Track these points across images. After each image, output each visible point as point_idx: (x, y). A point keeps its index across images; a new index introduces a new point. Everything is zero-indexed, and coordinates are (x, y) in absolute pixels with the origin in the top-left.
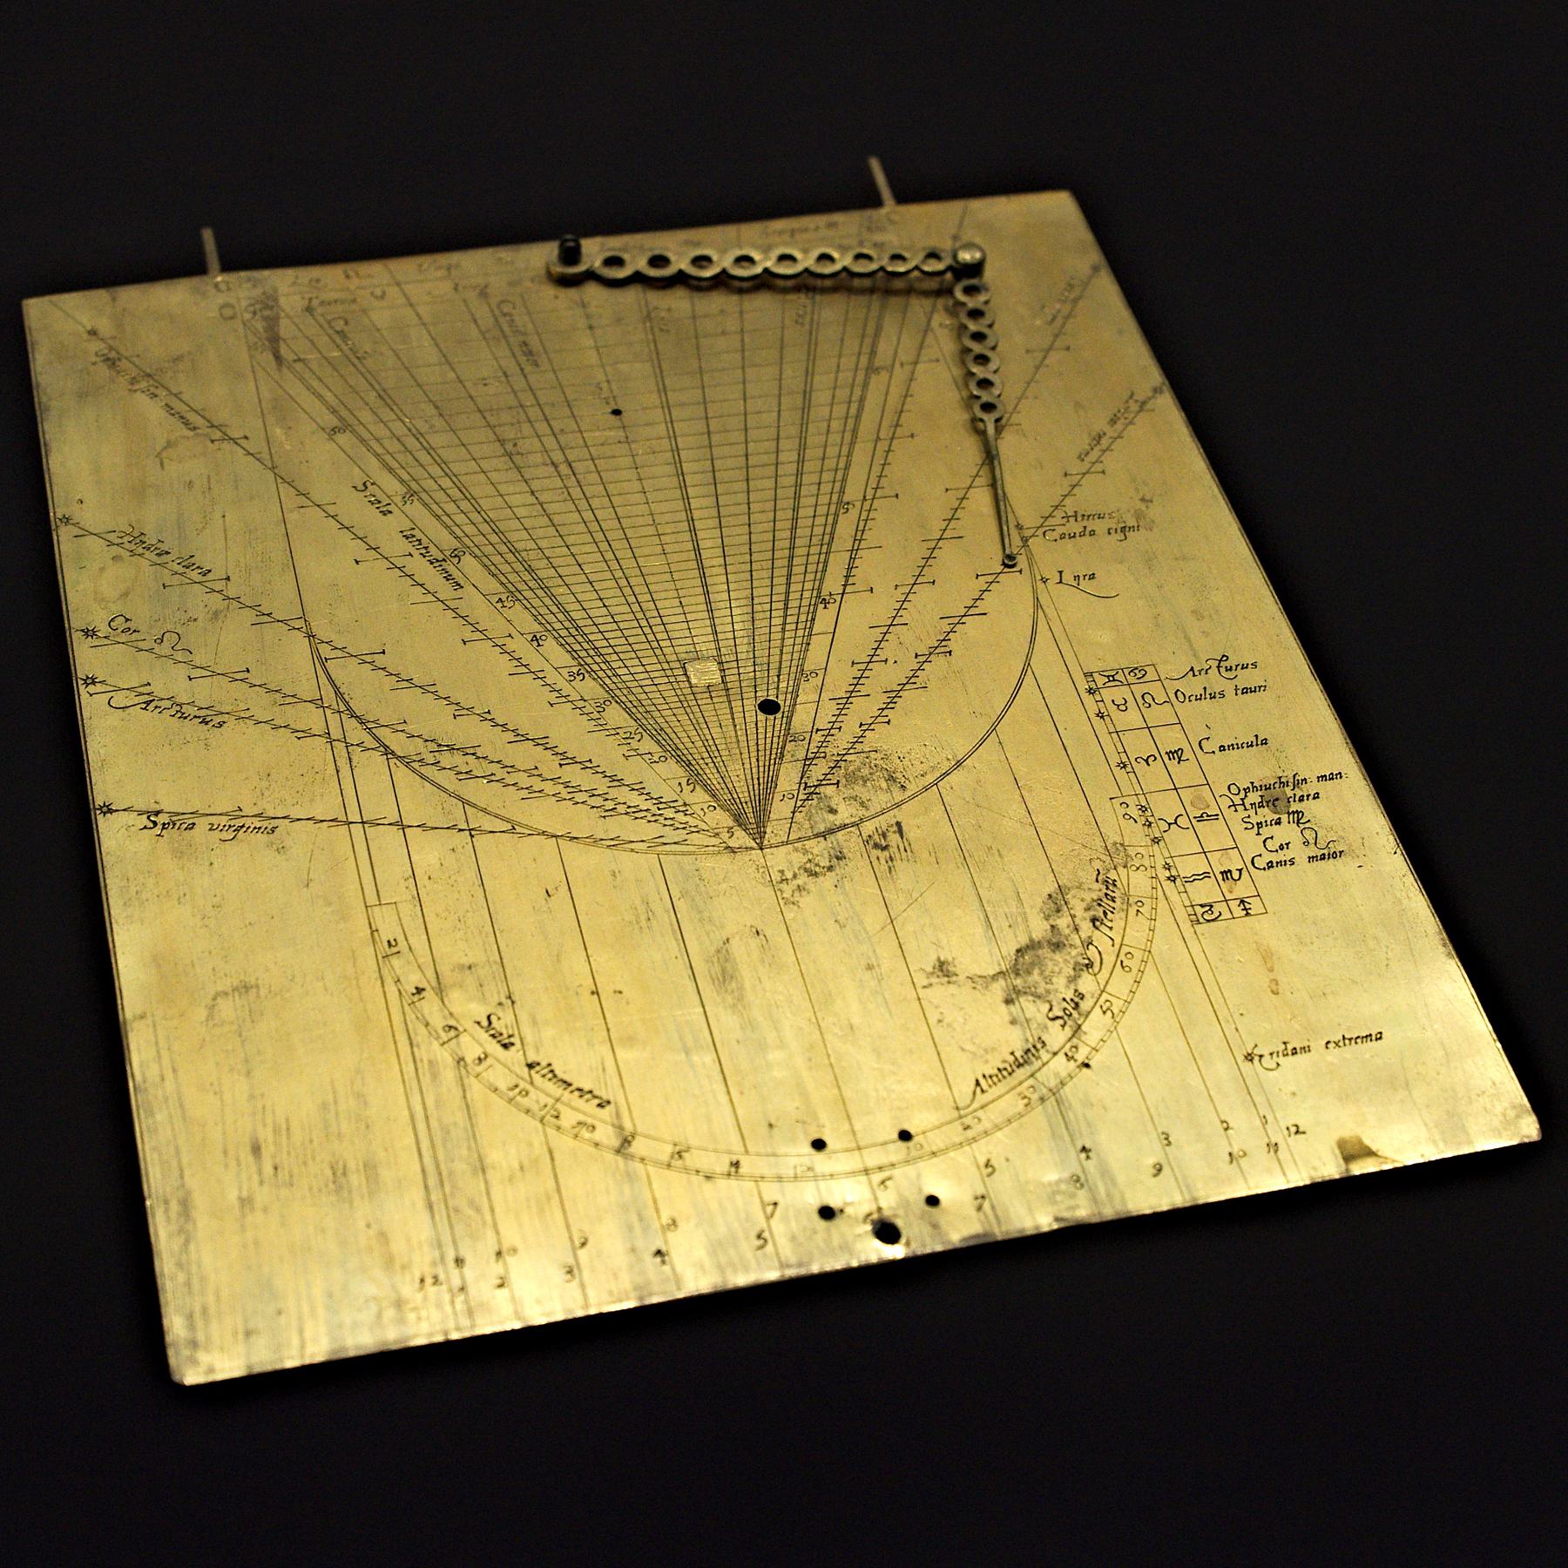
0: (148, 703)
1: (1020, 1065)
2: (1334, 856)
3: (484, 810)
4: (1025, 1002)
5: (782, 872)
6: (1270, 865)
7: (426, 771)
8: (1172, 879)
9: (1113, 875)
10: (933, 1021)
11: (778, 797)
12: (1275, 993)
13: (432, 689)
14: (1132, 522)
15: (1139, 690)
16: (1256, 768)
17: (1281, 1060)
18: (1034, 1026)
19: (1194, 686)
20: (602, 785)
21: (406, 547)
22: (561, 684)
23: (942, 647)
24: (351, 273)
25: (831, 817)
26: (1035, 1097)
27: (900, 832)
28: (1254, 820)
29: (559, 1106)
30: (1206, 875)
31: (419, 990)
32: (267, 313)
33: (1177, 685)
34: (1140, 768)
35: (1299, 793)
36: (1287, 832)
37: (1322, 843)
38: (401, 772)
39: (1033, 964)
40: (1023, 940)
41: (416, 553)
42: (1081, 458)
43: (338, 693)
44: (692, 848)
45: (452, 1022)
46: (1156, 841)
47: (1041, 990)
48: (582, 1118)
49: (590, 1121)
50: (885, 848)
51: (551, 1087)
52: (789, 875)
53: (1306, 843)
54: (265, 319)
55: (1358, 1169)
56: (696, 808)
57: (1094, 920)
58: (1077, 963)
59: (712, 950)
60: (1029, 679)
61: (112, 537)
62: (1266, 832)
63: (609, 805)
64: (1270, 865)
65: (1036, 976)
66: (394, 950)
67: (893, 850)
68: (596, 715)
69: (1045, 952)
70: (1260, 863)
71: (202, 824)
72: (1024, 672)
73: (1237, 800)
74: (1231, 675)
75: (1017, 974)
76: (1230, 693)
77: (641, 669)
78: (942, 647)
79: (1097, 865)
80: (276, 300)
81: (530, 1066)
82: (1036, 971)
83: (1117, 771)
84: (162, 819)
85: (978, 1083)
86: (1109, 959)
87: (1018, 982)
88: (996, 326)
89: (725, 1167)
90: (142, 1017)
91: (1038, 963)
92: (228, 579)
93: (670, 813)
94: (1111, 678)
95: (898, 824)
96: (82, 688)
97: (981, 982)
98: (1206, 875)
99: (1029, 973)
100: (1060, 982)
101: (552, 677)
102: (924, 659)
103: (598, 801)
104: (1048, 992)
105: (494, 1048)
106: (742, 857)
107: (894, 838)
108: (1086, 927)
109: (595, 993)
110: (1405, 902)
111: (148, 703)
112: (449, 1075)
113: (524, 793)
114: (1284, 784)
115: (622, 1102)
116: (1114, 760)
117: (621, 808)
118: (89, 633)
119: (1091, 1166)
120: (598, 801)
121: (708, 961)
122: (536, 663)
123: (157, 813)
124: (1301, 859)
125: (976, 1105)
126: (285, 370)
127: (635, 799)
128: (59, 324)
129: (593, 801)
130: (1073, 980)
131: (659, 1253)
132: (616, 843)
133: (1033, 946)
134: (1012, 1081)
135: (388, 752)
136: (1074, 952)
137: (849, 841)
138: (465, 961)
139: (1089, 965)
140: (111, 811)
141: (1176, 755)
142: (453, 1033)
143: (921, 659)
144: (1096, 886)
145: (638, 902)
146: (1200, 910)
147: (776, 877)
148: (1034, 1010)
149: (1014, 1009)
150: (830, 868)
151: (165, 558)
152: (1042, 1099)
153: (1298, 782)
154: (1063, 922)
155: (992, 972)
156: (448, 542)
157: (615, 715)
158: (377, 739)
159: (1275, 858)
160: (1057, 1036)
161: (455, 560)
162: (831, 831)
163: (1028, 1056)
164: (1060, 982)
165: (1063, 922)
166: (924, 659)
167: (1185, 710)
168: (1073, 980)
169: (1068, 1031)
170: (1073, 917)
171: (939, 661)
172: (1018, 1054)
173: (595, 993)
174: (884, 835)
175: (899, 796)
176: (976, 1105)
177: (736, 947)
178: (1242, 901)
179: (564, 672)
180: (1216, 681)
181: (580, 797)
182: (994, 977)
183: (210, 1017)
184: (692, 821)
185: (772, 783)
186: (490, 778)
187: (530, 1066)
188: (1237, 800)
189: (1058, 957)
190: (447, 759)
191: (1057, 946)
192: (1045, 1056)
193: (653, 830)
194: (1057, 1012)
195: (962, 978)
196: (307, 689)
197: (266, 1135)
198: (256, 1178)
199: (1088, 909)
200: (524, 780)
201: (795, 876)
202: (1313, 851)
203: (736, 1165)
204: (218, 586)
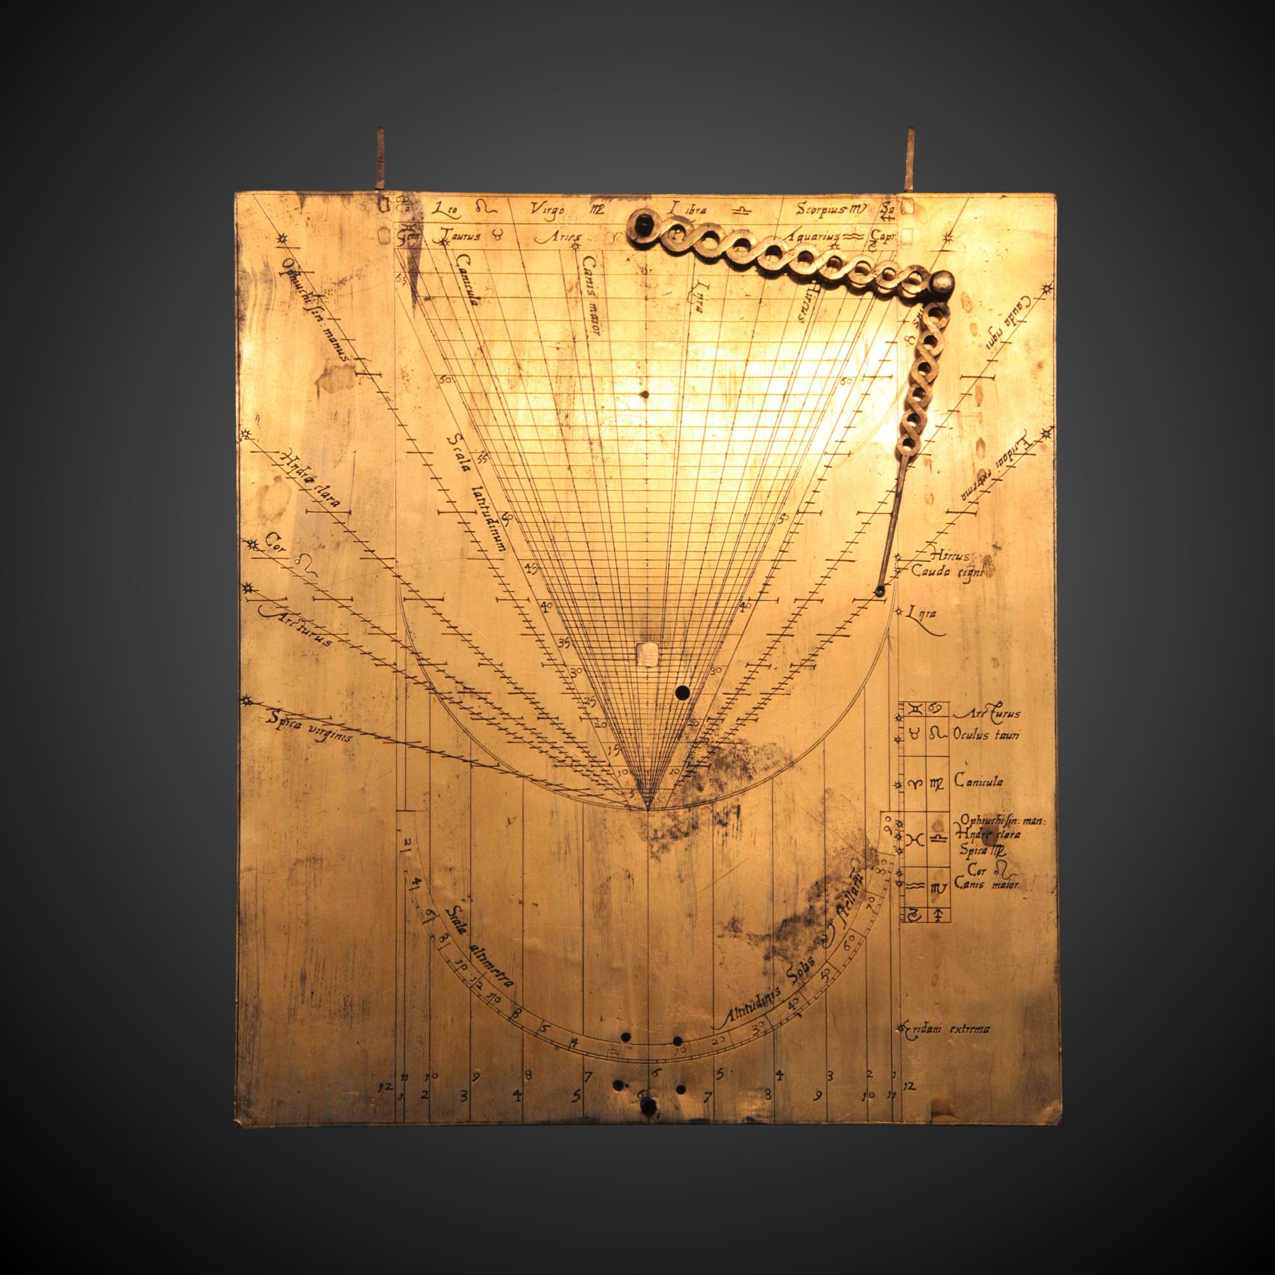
0: (284, 615)
1: (760, 1006)
2: (1011, 886)
3: (482, 747)
4: (777, 960)
5: (656, 831)
6: (966, 885)
7: (453, 708)
8: (899, 884)
9: (862, 874)
10: (717, 963)
11: (669, 770)
12: (934, 985)
13: (468, 638)
14: (979, 567)
15: (932, 722)
16: (985, 804)
17: (920, 1034)
18: (777, 977)
19: (969, 726)
20: (560, 739)
21: (473, 504)
22: (553, 649)
23: (809, 663)
24: (481, 204)
25: (698, 793)
26: (762, 1029)
27: (738, 813)
28: (969, 847)
29: (483, 980)
30: (921, 885)
31: (418, 881)
32: (412, 241)
33: (958, 723)
34: (909, 789)
35: (1007, 830)
36: (987, 860)
37: (1006, 874)
38: (437, 706)
39: (790, 933)
40: (790, 914)
41: (480, 511)
42: (964, 497)
43: (408, 632)
44: (606, 802)
45: (433, 908)
46: (900, 851)
47: (789, 953)
48: (495, 991)
49: (499, 995)
50: (725, 825)
51: (480, 965)
52: (660, 834)
53: (996, 872)
54: (410, 248)
55: (939, 1120)
56: (616, 769)
57: (839, 907)
58: (817, 938)
59: (599, 883)
60: (819, 749)
61: (276, 457)
62: (973, 858)
63: (562, 757)
64: (966, 885)
65: (789, 943)
66: (408, 847)
67: (729, 827)
68: (569, 680)
69: (800, 926)
70: (961, 882)
71: (306, 725)
72: (858, 695)
73: (964, 830)
74: (998, 720)
75: (778, 938)
76: (992, 736)
77: (607, 644)
78: (809, 663)
79: (855, 864)
80: (421, 229)
81: (472, 948)
82: (790, 939)
83: (893, 788)
84: (281, 716)
85: (731, 1014)
86: (838, 938)
87: (777, 944)
88: (940, 361)
89: (567, 1042)
90: (250, 869)
91: (793, 933)
92: (350, 513)
93: (598, 770)
94: (916, 709)
95: (739, 807)
96: (243, 592)
97: (755, 939)
98: (921, 885)
99: (786, 939)
100: (803, 949)
101: (548, 641)
102: (795, 669)
103: (555, 753)
104: (793, 956)
105: (453, 929)
106: (635, 815)
107: (733, 817)
108: (832, 910)
109: (521, 903)
110: (1044, 932)
111: (284, 615)
112: (423, 945)
113: (510, 738)
114: (999, 820)
115: (519, 983)
116: (895, 779)
117: (569, 761)
118: (252, 544)
119: (779, 1084)
120: (555, 753)
121: (594, 892)
122: (541, 629)
123: (279, 710)
124: (988, 886)
125: (724, 1029)
126: (419, 314)
127: (579, 755)
128: (261, 216)
129: (552, 752)
130: (811, 949)
131: (517, 1093)
132: (559, 789)
133: (795, 919)
134: (751, 1015)
135: (432, 689)
136: (818, 929)
137: (704, 815)
138: (449, 865)
139: (825, 941)
140: (250, 703)
141: (936, 782)
142: (432, 916)
143: (794, 668)
144: (849, 880)
145: (562, 839)
146: (908, 911)
147: (652, 834)
148: (779, 965)
149: (769, 964)
150: (687, 835)
151: (309, 485)
152: (766, 1032)
153: (1011, 821)
154: (819, 904)
155: (763, 933)
156: (503, 506)
157: (581, 682)
158: (426, 675)
159: (971, 879)
160: (788, 989)
161: (505, 523)
162: (695, 805)
163: (764, 1001)
164: (803, 949)
165: (819, 904)
166: (795, 669)
167: (958, 745)
168: (811, 949)
169: (796, 987)
170: (826, 901)
171: (805, 672)
172: (761, 997)
173: (521, 903)
174: (727, 814)
175: (745, 784)
176: (724, 1029)
177: (614, 884)
178: (938, 911)
179: (557, 638)
180: (986, 725)
181: (545, 747)
182: (763, 938)
183: (290, 877)
184: (611, 780)
185: (668, 759)
186: (490, 721)
187: (472, 948)
188: (964, 830)
189: (807, 931)
190: (468, 701)
191: (809, 922)
192: (777, 1002)
193: (582, 783)
194: (794, 972)
195: (744, 935)
196: (388, 626)
197: (310, 969)
198: (300, 998)
199: (837, 898)
200: (510, 725)
201: (663, 837)
202: (998, 879)
203: (575, 1042)
204: (343, 518)
